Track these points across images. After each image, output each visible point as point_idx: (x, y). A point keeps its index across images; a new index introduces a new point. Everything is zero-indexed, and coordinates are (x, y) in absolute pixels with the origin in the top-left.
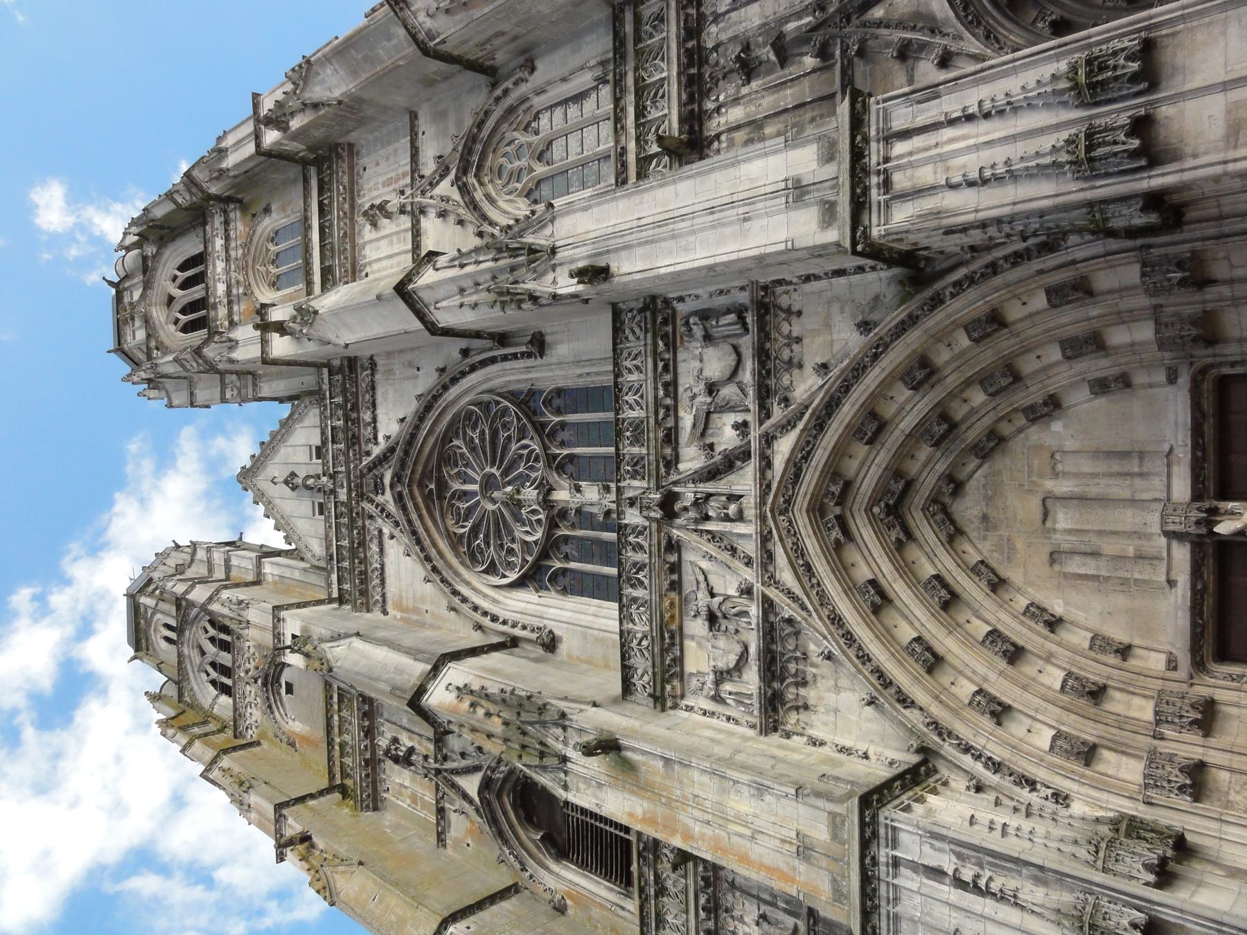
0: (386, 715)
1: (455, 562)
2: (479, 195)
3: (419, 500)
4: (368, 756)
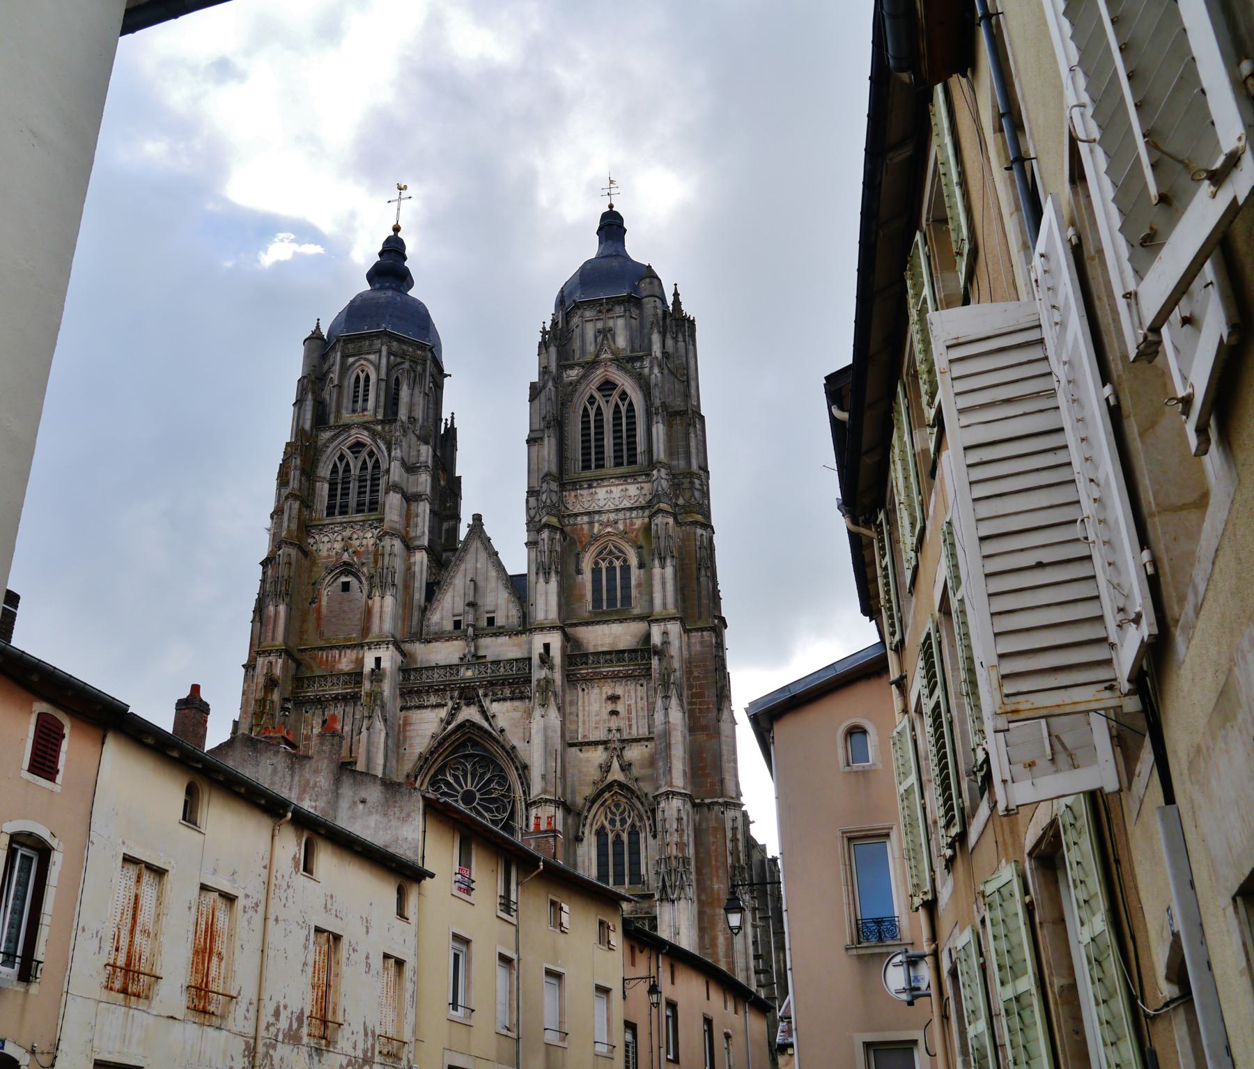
0: (347, 709)
1: (432, 772)
2: (607, 795)
3: (463, 739)
4: (323, 699)
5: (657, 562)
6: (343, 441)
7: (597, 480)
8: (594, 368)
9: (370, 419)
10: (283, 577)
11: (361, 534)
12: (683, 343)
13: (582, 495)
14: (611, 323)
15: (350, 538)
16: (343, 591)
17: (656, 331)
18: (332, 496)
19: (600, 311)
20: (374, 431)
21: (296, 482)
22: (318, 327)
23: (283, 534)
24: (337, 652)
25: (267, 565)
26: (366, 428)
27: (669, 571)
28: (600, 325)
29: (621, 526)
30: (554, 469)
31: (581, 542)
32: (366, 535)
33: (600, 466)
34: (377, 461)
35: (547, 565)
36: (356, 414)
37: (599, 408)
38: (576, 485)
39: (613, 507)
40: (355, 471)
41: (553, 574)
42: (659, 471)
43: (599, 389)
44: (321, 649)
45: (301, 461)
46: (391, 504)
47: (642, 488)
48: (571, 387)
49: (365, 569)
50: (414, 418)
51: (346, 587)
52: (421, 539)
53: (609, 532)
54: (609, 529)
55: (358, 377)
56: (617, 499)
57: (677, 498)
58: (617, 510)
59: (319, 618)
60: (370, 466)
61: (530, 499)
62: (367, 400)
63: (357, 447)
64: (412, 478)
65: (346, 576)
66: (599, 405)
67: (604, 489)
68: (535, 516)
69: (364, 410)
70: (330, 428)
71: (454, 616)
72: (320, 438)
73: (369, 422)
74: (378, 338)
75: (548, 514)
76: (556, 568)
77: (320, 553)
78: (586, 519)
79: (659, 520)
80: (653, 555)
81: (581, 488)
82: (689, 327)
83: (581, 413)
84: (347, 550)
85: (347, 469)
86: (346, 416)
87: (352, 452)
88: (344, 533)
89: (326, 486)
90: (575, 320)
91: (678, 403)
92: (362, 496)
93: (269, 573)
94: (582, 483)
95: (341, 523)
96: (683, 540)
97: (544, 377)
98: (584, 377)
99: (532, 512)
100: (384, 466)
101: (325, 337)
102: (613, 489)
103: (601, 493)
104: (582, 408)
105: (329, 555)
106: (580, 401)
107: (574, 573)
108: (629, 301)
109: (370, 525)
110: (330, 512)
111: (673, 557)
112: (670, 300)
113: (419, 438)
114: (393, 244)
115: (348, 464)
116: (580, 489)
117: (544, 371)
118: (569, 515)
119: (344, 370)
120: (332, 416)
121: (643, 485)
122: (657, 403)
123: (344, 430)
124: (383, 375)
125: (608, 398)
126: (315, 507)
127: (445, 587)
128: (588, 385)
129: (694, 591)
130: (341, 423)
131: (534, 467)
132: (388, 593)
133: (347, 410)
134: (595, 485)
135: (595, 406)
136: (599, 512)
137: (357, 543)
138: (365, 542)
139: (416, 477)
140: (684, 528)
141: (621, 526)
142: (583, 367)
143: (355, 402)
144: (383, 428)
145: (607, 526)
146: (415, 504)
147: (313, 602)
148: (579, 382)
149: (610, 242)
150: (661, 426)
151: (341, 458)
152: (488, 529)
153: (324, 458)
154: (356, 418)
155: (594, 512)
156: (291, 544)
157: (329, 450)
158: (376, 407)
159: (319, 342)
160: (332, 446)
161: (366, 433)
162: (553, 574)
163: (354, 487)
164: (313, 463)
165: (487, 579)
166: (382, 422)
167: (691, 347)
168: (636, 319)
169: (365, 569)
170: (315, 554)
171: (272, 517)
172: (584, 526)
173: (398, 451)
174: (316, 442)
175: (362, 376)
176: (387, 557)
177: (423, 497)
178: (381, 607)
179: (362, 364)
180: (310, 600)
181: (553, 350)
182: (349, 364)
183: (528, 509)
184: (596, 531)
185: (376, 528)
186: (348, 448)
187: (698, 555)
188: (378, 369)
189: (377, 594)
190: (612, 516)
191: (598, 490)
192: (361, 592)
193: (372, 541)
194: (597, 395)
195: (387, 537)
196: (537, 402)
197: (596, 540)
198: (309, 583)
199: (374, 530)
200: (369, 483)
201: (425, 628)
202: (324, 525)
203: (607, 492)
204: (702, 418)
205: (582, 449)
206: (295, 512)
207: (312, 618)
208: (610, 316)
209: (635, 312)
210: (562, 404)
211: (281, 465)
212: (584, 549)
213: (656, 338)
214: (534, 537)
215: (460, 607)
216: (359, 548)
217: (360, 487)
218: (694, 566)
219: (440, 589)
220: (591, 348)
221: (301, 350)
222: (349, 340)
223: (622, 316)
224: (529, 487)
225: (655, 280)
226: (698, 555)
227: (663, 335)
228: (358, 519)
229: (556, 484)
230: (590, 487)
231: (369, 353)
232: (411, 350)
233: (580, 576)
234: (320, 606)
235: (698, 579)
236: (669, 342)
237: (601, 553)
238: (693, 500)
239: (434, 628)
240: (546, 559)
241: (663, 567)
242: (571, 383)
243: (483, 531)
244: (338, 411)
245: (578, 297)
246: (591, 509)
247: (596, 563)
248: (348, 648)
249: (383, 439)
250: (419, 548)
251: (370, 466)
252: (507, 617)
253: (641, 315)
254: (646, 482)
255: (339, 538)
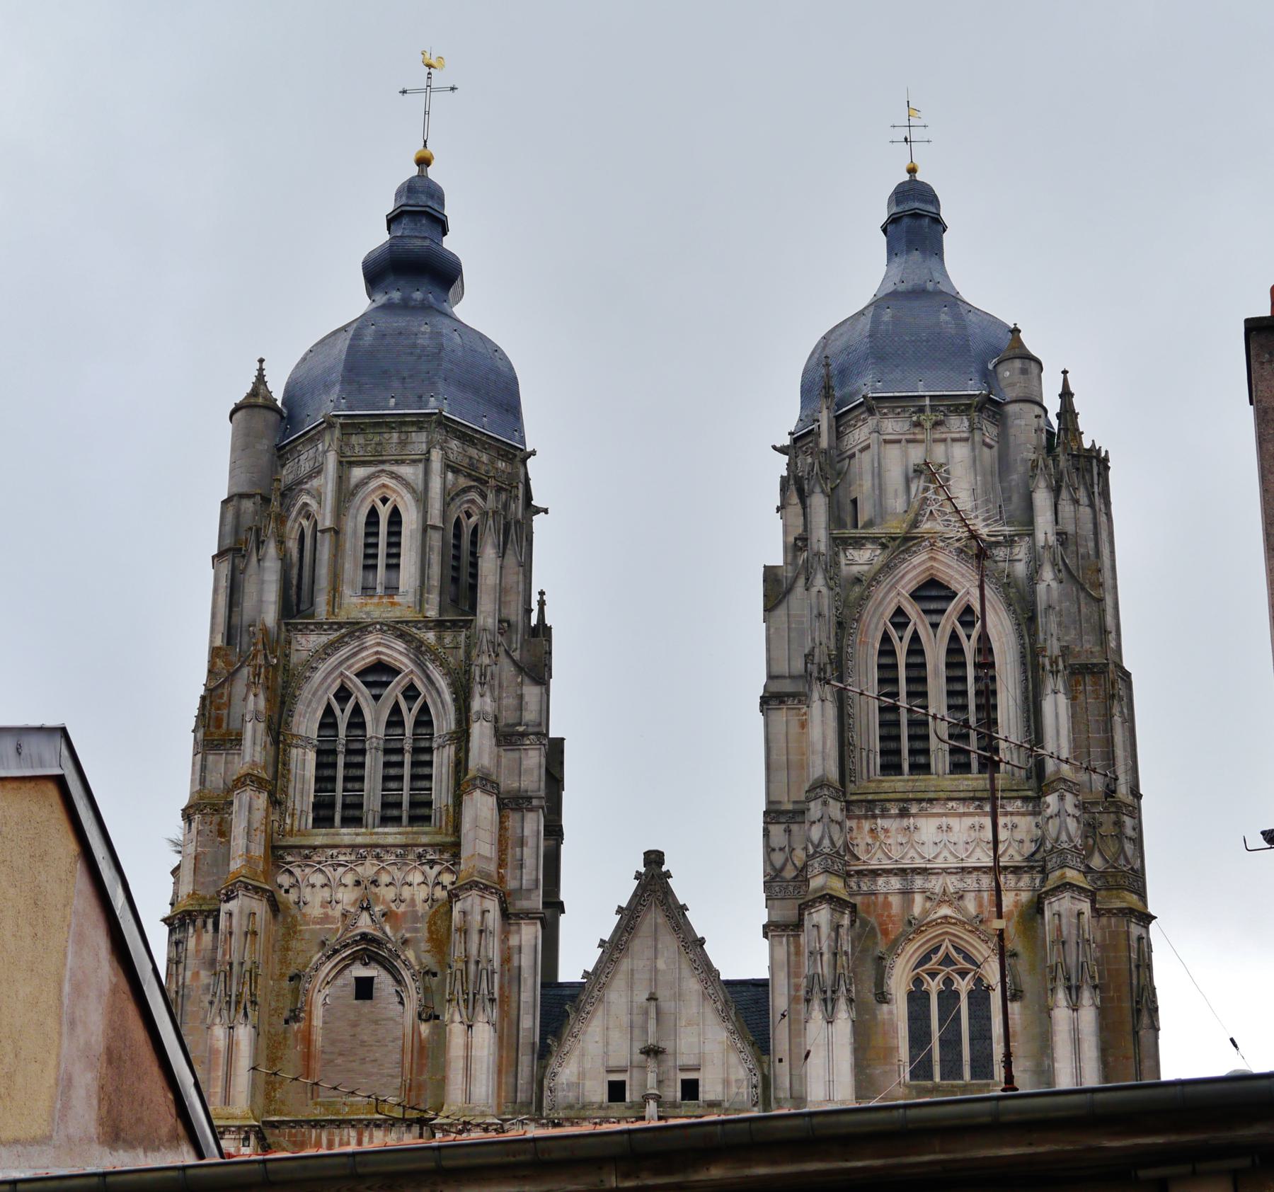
5: (1061, 995)
6: (348, 659)
7: (920, 801)
8: (907, 551)
9: (410, 615)
10: (242, 964)
11: (398, 875)
12: (1088, 510)
13: (886, 831)
14: (939, 453)
15: (375, 883)
16: (357, 998)
17: (1042, 484)
18: (324, 781)
19: (918, 424)
20: (421, 643)
21: (258, 748)
22: (261, 378)
23: (236, 865)
24: (353, 1133)
25: (183, 925)
26: (402, 636)
27: (1088, 1016)
28: (916, 455)
29: (970, 905)
30: (833, 773)
31: (885, 933)
32: (410, 879)
33: (921, 768)
34: (425, 709)
35: (829, 982)
36: (375, 600)
37: (915, 638)
38: (872, 807)
39: (953, 863)
40: (375, 728)
41: (842, 1005)
42: (1062, 798)
43: (916, 596)
44: (317, 1124)
45: (267, 700)
46: (476, 819)
47: (1015, 826)
48: (857, 589)
49: (410, 954)
50: (508, 622)
51: (364, 989)
52: (533, 896)
53: (946, 917)
54: (945, 911)
55: (373, 513)
56: (961, 846)
57: (1090, 855)
58: (963, 869)
59: (307, 1057)
60: (409, 720)
61: (772, 828)
62: (397, 566)
63: (378, 673)
64: (508, 757)
65: (366, 964)
66: (915, 632)
67: (935, 822)
68: (784, 865)
69: (392, 589)
70: (319, 625)
71: (609, 1071)
72: (294, 646)
73: (407, 622)
74: (421, 429)
75: (826, 871)
76: (848, 991)
77: (306, 910)
78: (896, 883)
79: (1064, 905)
80: (1054, 979)
81: (884, 815)
82: (1099, 474)
83: (877, 646)
84: (367, 909)
85: (357, 721)
86: (353, 605)
87: (367, 684)
88: (359, 869)
89: (311, 757)
90: (859, 435)
91: (1087, 646)
92: (392, 785)
93: (191, 943)
94: (888, 805)
95: (353, 847)
96: (1103, 947)
97: (795, 557)
98: (887, 568)
99: (778, 859)
100: (444, 722)
101: (279, 403)
102: (954, 822)
103: (927, 828)
104: (879, 635)
105: (326, 914)
106: (876, 620)
107: (871, 998)
108: (980, 409)
109: (420, 856)
110: (323, 816)
111: (1095, 987)
112: (1053, 405)
113: (520, 668)
114: (423, 199)
115: (357, 710)
116: (883, 816)
117: (798, 544)
118: (859, 873)
119: (345, 494)
120: (322, 601)
121: (1016, 819)
122: (1054, 647)
123: (350, 634)
124: (435, 518)
125: (935, 618)
126: (290, 804)
127: (588, 1008)
128: (893, 587)
129: (1127, 1058)
130: (342, 617)
131: (780, 758)
132: (481, 1018)
133: (353, 583)
134: (914, 809)
135: (908, 633)
136: (924, 871)
137: (389, 893)
138: (406, 892)
139: (515, 755)
140: (1104, 920)
141: (970, 905)
142: (884, 546)
143: (370, 568)
144: (440, 639)
145: (941, 902)
146: (517, 816)
147: (296, 1018)
148: (875, 579)
149: (916, 256)
150: (1062, 700)
151: (343, 694)
152: (680, 888)
153: (306, 693)
154: (375, 610)
155: (914, 870)
156: (257, 890)
157: (318, 676)
158: (423, 587)
159: (272, 417)
160: (324, 668)
161: (400, 645)
162: (842, 1005)
163: (373, 764)
164: (283, 703)
165: (679, 996)
166: (439, 625)
167: (1103, 519)
168: (990, 447)
169: (410, 954)
170: (294, 910)
171: (187, 815)
172: (891, 898)
173: (488, 699)
174: (287, 656)
175: (384, 512)
176: (475, 937)
177: (535, 802)
178: (468, 1047)
179: (384, 486)
180: (286, 1014)
181: (819, 503)
182: (354, 481)
183: (769, 850)
184: (917, 910)
185: (432, 863)
186: (357, 675)
187: (1135, 982)
188: (422, 500)
189: (457, 1018)
190: (953, 883)
191: (921, 822)
192: (402, 1003)
193: (422, 893)
194: (912, 610)
195: (474, 892)
196: (781, 612)
197: (919, 932)
198: (282, 975)
199: (426, 868)
200: (407, 758)
201: (546, 1093)
202: (315, 848)
203: (940, 828)
204: (1127, 676)
205: (881, 725)
206: (259, 816)
207: (293, 1054)
208: (937, 436)
209: (990, 432)
210: (840, 625)
211: (203, 698)
212: (894, 947)
213: (1042, 499)
214: (788, 912)
215: (622, 1051)
216: (393, 906)
217: (387, 765)
218: (1127, 1005)
219: (578, 1010)
220: (897, 504)
221: (223, 434)
222: (352, 426)
223: (966, 440)
224: (769, 802)
225: (1033, 364)
226: (1135, 982)
227: (1056, 491)
228: (390, 840)
229: (839, 805)
230: (904, 814)
231: (398, 462)
232: (485, 458)
233: (885, 1007)
234: (310, 1026)
235: (1136, 1033)
236: (1066, 508)
237: (926, 959)
238: (1122, 862)
239: (564, 1095)
240: (825, 970)
241: (1075, 1008)
242: (858, 580)
243: (668, 892)
244: (335, 590)
245: (867, 385)
246: (906, 863)
247: (918, 981)
248: (378, 1126)
249: (437, 659)
250: (528, 915)
251: (409, 720)
252: (726, 1083)
253: (1003, 437)
254: (1023, 814)
255: (349, 879)
